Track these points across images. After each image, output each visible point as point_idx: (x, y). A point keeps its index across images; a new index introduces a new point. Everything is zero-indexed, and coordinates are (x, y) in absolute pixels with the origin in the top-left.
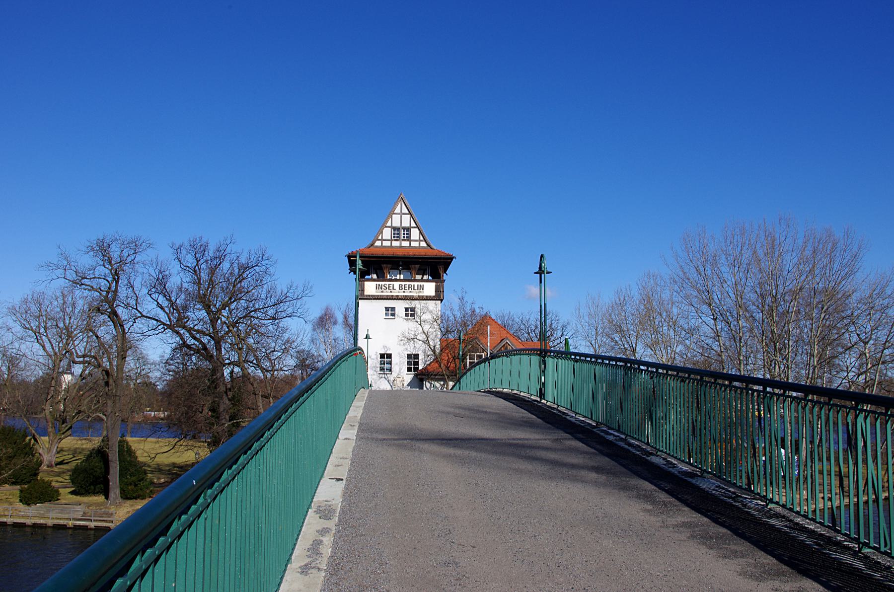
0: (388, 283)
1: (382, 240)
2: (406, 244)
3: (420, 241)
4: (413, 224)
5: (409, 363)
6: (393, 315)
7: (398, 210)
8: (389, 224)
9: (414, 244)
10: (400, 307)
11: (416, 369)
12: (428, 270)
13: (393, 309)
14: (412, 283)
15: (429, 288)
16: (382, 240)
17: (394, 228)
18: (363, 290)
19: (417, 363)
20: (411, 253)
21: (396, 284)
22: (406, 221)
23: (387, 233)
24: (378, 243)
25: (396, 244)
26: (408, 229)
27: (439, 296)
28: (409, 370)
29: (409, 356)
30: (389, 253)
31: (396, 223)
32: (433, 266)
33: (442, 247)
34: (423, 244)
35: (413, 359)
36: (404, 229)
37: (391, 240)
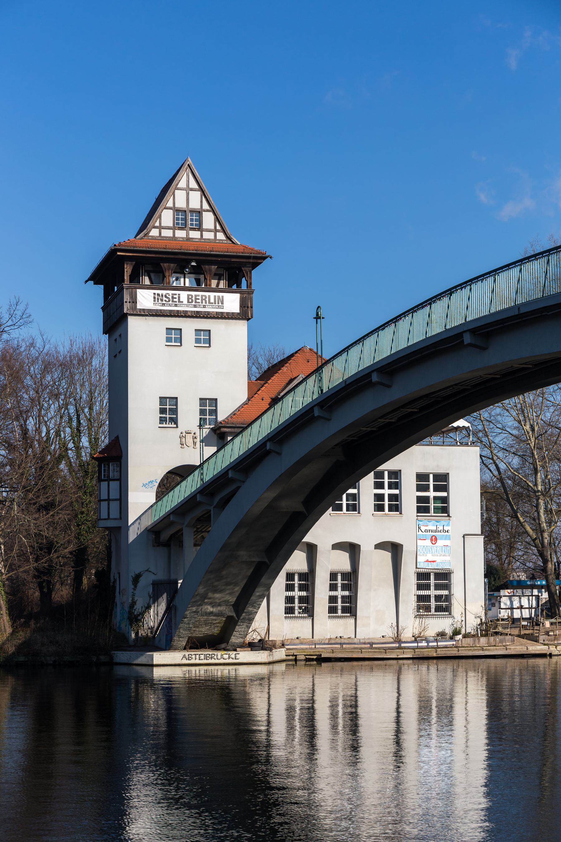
0: (171, 292)
1: (160, 228)
2: (195, 235)
3: (216, 231)
4: (206, 206)
7: (182, 184)
8: (170, 204)
9: (206, 235)
10: (189, 327)
12: (226, 275)
14: (207, 294)
15: (232, 302)
17: (177, 211)
19: (214, 412)
20: (206, 249)
21: (184, 295)
22: (196, 201)
23: (167, 217)
24: (154, 233)
26: (199, 213)
27: (245, 314)
30: (173, 247)
31: (181, 203)
32: (233, 268)
34: (221, 236)
35: (208, 405)
36: (192, 211)
37: (174, 228)
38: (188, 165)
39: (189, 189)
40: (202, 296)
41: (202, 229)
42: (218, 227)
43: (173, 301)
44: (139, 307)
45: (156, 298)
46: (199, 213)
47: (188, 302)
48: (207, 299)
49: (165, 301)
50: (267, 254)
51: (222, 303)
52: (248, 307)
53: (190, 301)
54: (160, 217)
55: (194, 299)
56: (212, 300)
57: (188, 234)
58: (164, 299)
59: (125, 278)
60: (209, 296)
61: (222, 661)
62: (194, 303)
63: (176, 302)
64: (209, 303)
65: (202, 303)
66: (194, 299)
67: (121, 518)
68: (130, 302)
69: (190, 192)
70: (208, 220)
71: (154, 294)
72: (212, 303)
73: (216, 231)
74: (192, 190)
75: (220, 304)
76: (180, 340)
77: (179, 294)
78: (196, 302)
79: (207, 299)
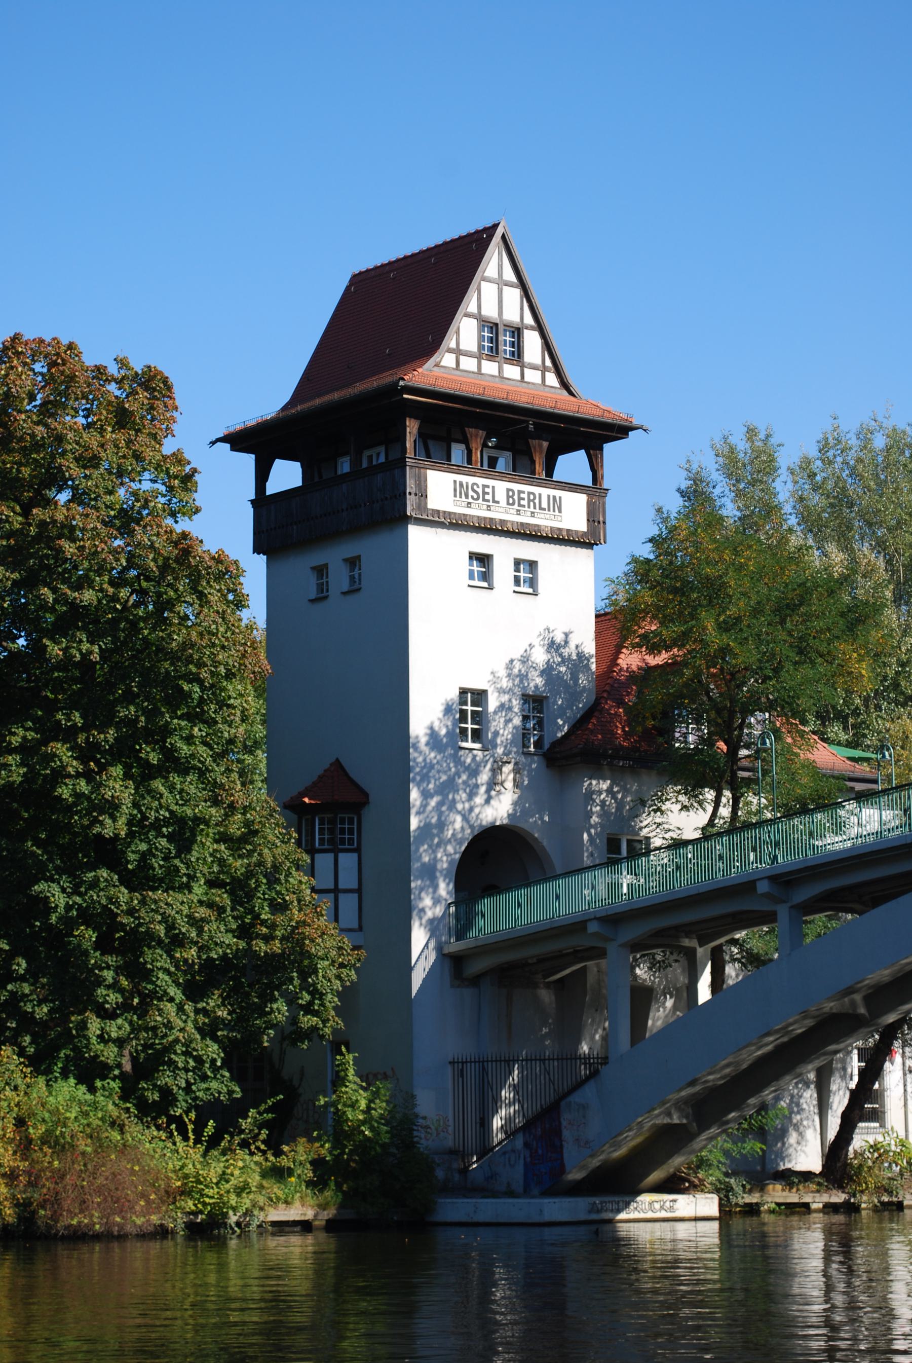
2: (512, 372)
4: (529, 320)
8: (472, 308)
10: (504, 552)
13: (532, 565)
22: (513, 308)
25: (490, 368)
26: (517, 332)
31: (490, 311)
33: (596, 398)
34: (552, 379)
38: (503, 237)
39: (501, 283)
40: (529, 493)
41: (523, 363)
42: (548, 363)
43: (484, 500)
45: (460, 490)
46: (517, 332)
47: (508, 503)
48: (537, 501)
49: (472, 497)
50: (636, 422)
51: (560, 511)
52: (599, 522)
53: (511, 501)
54: (458, 332)
55: (516, 497)
56: (544, 505)
57: (500, 369)
58: (471, 493)
59: (408, 445)
60: (540, 495)
61: (650, 1215)
62: (516, 506)
63: (488, 501)
64: (541, 508)
65: (529, 507)
66: (516, 497)
67: (360, 928)
68: (416, 495)
69: (504, 287)
71: (455, 482)
72: (544, 509)
73: (544, 370)
74: (508, 284)
75: (557, 512)
76: (486, 576)
77: (493, 487)
78: (520, 505)
79: (537, 501)
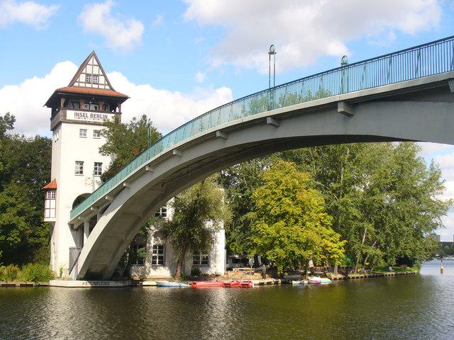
0: (83, 112)
1: (79, 82)
4: (101, 73)
5: (96, 169)
6: (85, 135)
7: (90, 62)
8: (84, 71)
9: (101, 87)
11: (100, 173)
14: (100, 114)
16: (79, 82)
17: (88, 75)
18: (66, 116)
20: (100, 93)
21: (89, 113)
22: (96, 70)
23: (82, 78)
25: (88, 85)
28: (96, 173)
29: (96, 164)
34: (107, 87)
36: (95, 75)
44: (68, 118)
70: (102, 80)
